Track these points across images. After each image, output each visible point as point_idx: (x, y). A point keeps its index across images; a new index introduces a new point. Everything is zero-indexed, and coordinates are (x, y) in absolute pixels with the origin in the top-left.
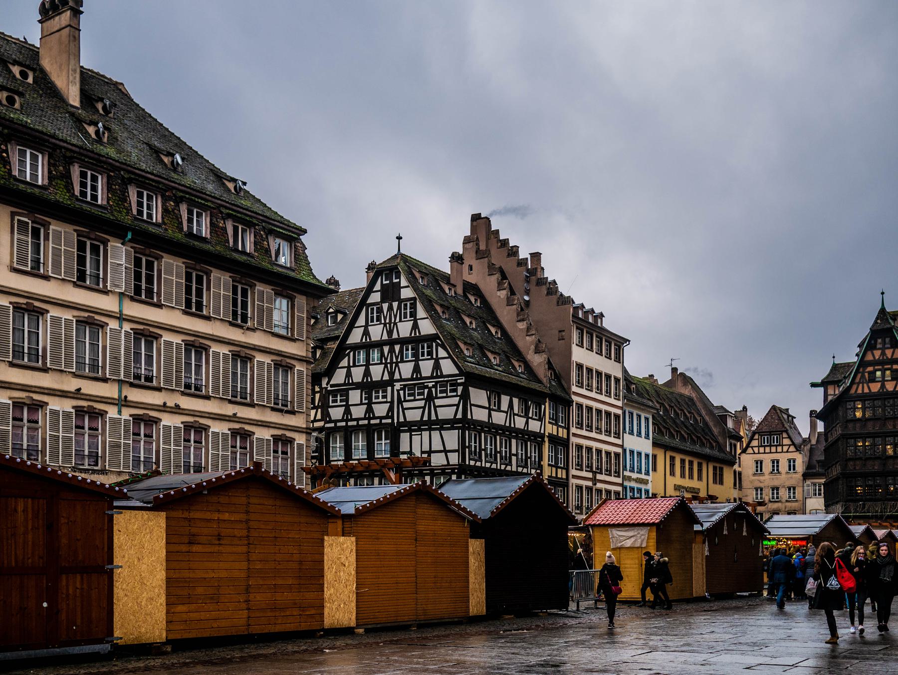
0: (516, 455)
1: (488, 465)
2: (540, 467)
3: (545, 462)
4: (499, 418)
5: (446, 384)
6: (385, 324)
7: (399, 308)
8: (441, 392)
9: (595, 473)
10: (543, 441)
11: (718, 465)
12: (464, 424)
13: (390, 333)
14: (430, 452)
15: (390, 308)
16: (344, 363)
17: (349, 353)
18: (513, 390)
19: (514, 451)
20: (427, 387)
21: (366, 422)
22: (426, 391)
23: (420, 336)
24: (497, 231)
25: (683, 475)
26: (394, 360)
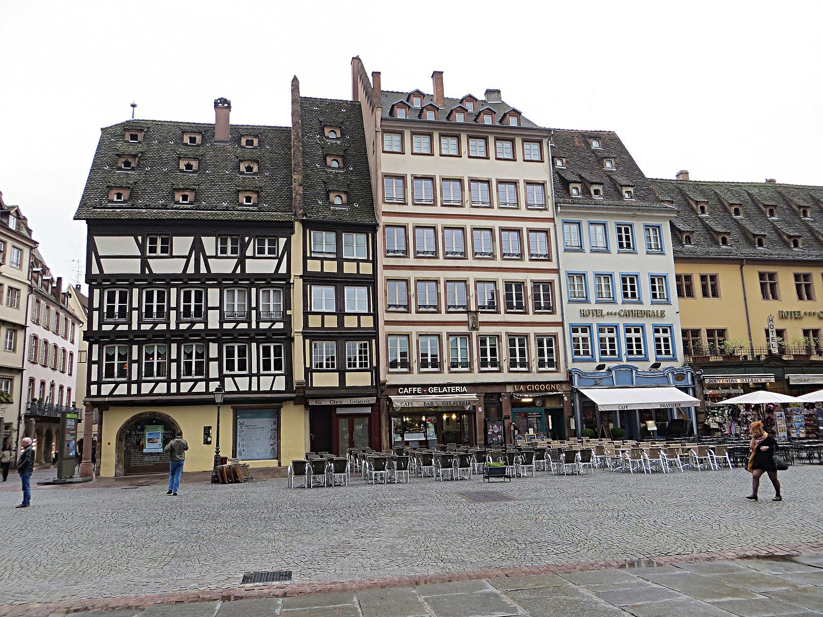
18: (195, 227)
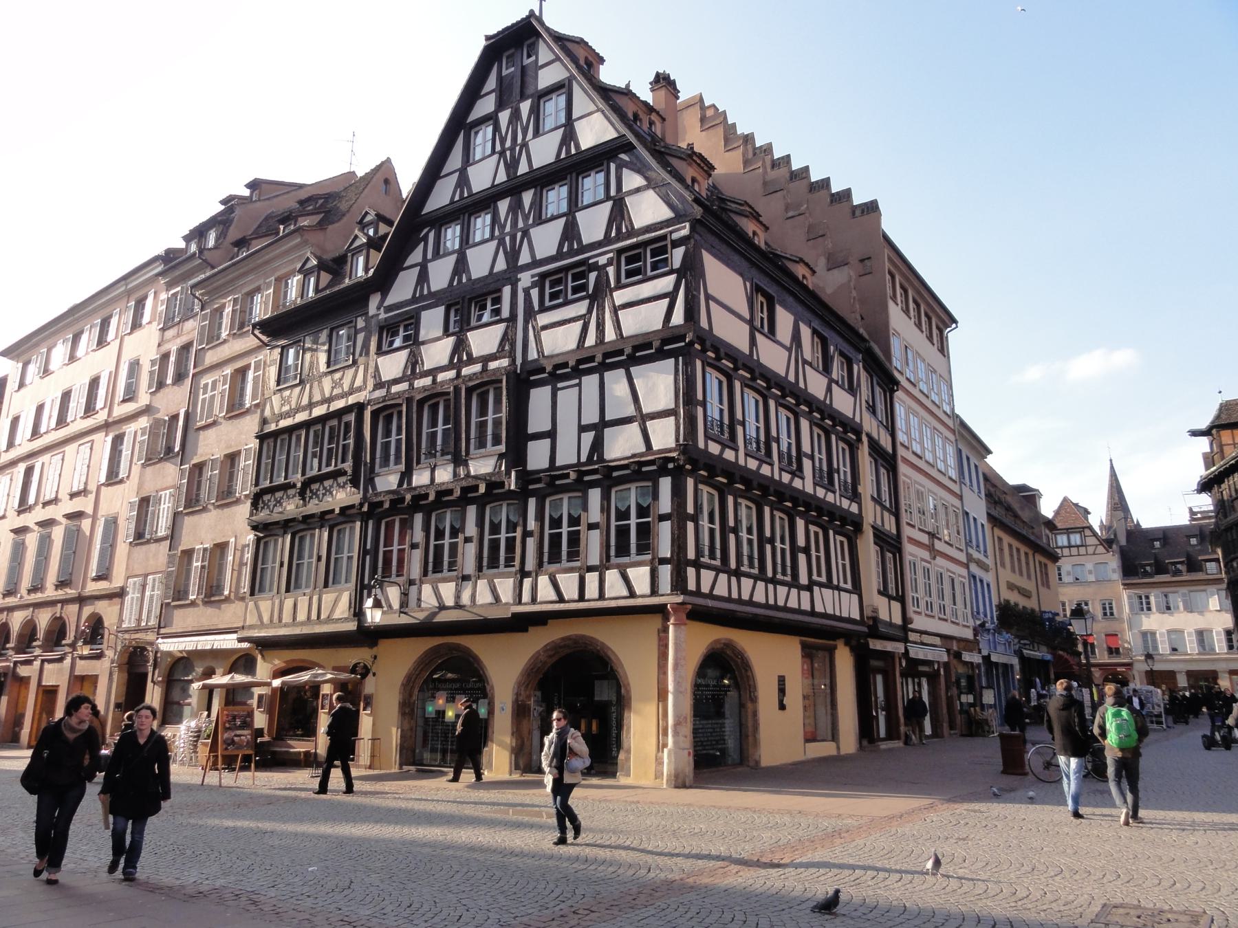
0: (812, 457)
1: (752, 464)
2: (855, 496)
3: (867, 487)
4: (773, 357)
5: (643, 254)
6: (502, 153)
7: (535, 111)
8: (629, 274)
9: (932, 536)
10: (859, 440)
11: (1044, 560)
12: (686, 345)
13: (512, 166)
14: (603, 424)
15: (516, 115)
16: (416, 257)
17: (427, 235)
19: (806, 448)
20: (595, 267)
21: (451, 374)
22: (593, 276)
23: (579, 152)
24: (734, 124)
25: (1013, 571)
26: (521, 224)
